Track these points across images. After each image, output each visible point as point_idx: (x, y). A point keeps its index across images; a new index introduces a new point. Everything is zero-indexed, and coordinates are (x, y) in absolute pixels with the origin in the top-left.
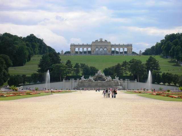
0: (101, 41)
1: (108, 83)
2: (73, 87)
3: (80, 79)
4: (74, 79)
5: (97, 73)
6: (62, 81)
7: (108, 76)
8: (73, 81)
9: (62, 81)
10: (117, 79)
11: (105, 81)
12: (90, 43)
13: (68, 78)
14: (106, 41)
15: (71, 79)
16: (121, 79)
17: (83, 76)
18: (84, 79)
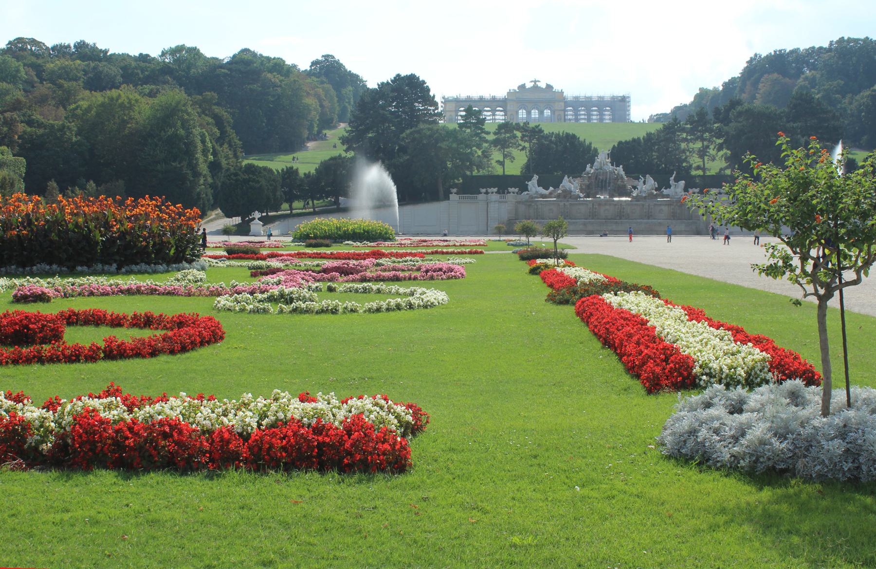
0: (536, 88)
1: (643, 205)
2: (494, 225)
3: (524, 188)
4: (495, 190)
5: (592, 163)
6: (447, 198)
7: (644, 177)
8: (495, 197)
9: (447, 198)
10: (677, 188)
11: (628, 195)
12: (501, 93)
13: (471, 187)
14: (549, 87)
15: (484, 190)
16: (691, 191)
17: (536, 178)
18: (541, 190)
